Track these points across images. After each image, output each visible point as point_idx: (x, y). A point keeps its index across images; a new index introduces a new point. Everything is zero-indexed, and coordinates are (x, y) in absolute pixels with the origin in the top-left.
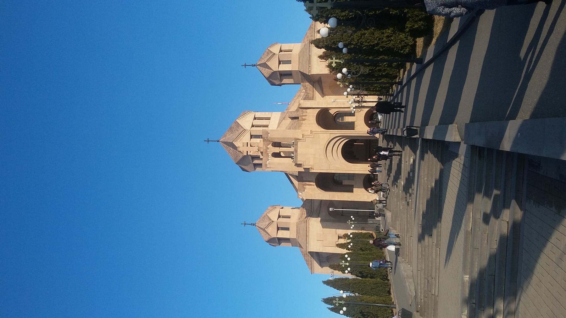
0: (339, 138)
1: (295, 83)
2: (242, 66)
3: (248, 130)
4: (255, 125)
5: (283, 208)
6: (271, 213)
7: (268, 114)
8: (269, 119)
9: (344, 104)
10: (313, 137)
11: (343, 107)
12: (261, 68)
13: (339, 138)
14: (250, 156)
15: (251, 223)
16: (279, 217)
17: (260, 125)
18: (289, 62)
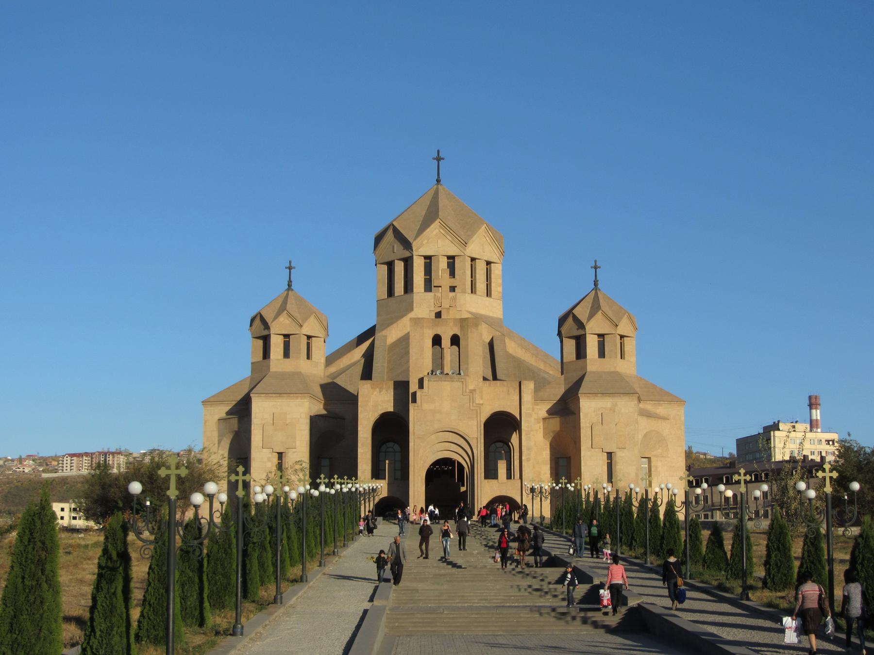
0: (470, 453)
1: (564, 365)
2: (595, 262)
3: (465, 250)
4: (475, 264)
5: (325, 342)
6: (316, 322)
7: (497, 291)
8: (489, 293)
9: (528, 460)
10: (471, 407)
11: (523, 458)
12: (590, 300)
13: (470, 453)
14: (411, 255)
15: (292, 279)
16: (309, 337)
17: (475, 276)
18: (602, 354)
